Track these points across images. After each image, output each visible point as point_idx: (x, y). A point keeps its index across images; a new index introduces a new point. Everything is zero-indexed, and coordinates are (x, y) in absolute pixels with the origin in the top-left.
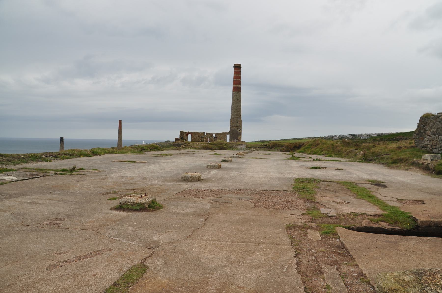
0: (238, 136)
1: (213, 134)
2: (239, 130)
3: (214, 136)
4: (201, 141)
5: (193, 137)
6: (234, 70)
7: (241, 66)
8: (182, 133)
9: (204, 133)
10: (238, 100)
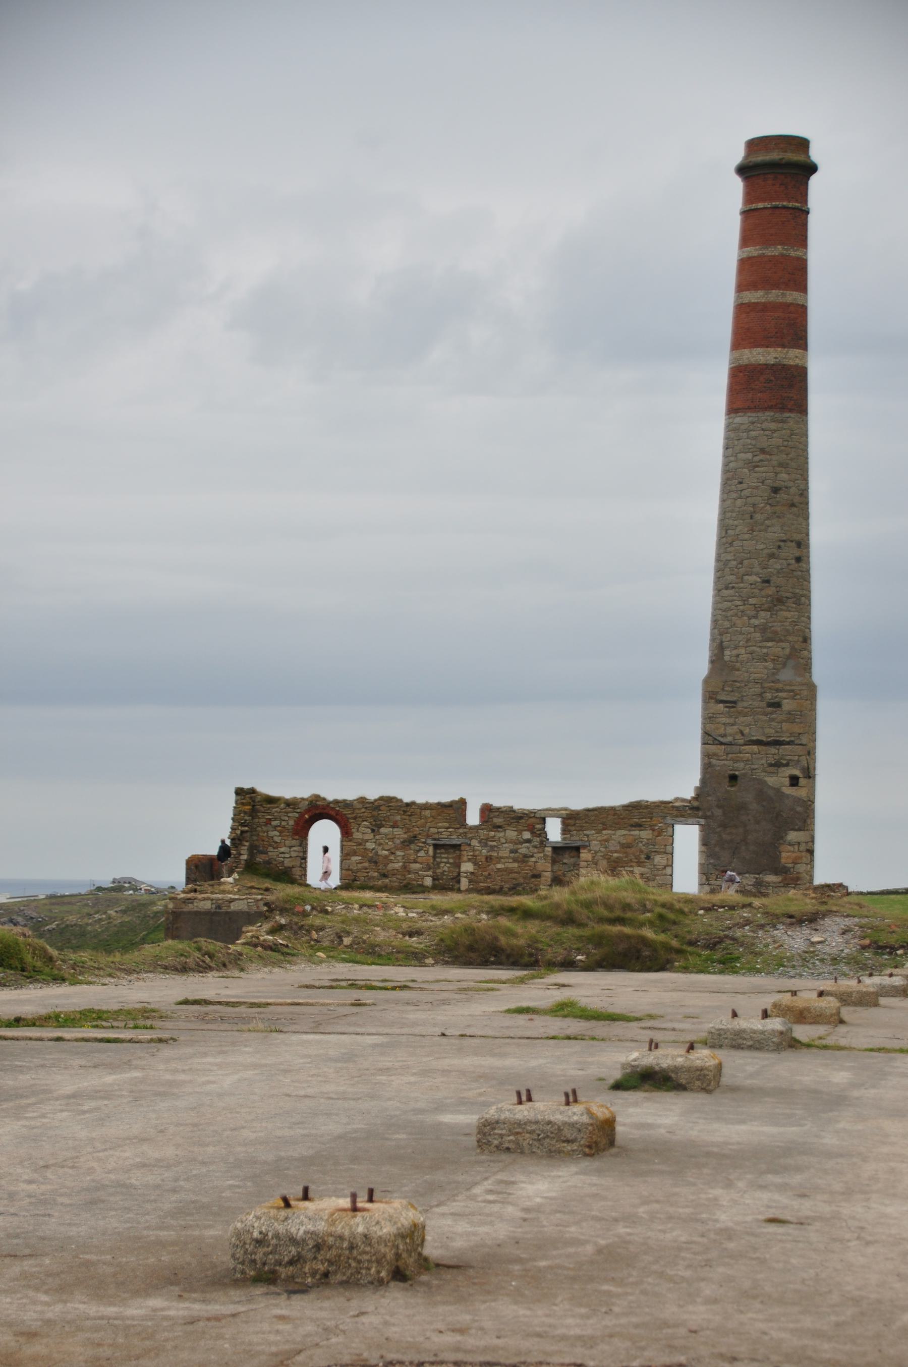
1: (543, 820)
3: (554, 831)
4: (428, 882)
6: (749, 197)
7: (816, 154)
10: (776, 490)
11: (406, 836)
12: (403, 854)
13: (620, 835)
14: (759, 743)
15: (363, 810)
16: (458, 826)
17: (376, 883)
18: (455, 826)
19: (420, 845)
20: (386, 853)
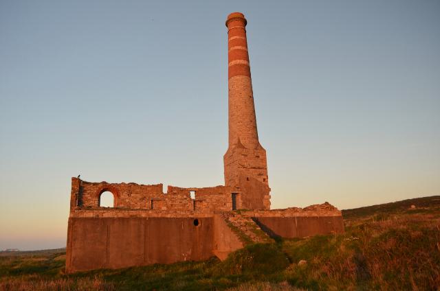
0: (262, 197)
2: (264, 180)
5: (123, 200)
8: (81, 188)
9: (160, 186)
13: (216, 197)
14: (254, 168)
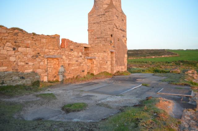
11: (34, 53)
12: (33, 64)
15: (7, 34)
16: (58, 49)
17: (18, 84)
18: (57, 49)
19: (42, 58)
20: (23, 64)
